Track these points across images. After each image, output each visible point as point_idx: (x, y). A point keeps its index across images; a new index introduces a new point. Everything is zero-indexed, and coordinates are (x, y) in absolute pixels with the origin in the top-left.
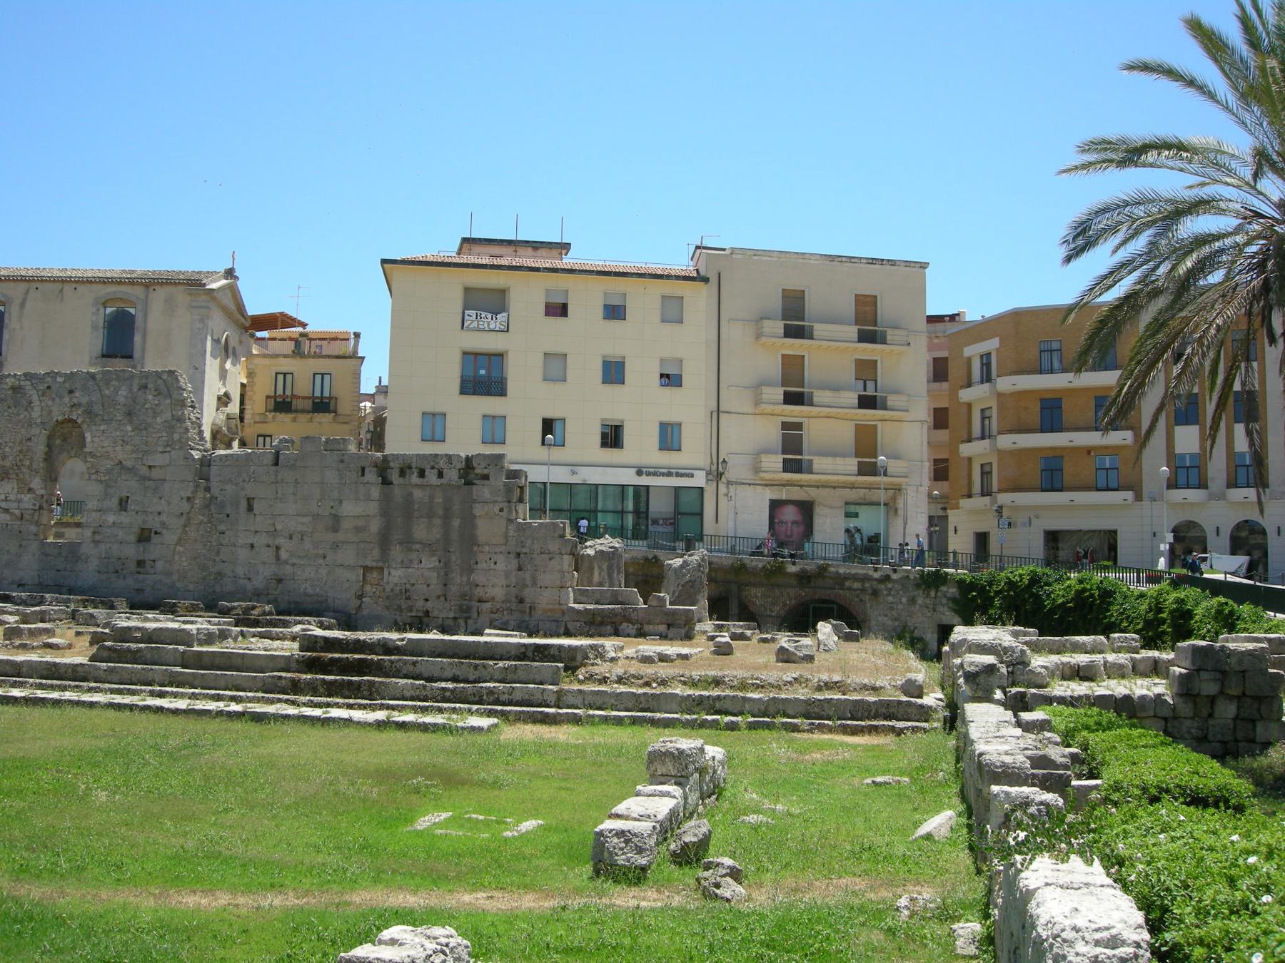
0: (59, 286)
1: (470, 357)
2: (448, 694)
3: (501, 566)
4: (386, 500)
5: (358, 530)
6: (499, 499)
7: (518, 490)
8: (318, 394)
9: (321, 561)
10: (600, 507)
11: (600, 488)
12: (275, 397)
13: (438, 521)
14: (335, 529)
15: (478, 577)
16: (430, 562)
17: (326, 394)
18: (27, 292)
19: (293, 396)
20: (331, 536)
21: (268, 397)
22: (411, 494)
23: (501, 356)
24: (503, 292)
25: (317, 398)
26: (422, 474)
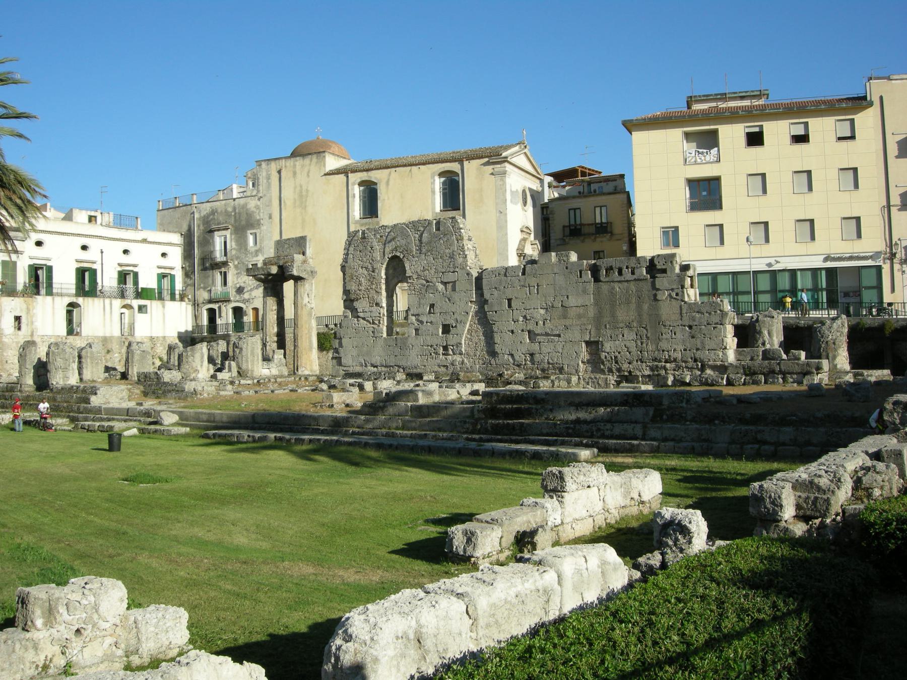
0: (409, 168)
1: (694, 184)
2: (570, 431)
3: (679, 335)
4: (597, 294)
5: (579, 316)
6: (674, 287)
7: (689, 279)
8: (572, 222)
9: (556, 338)
10: (799, 287)
11: (799, 273)
12: (570, 226)
13: (633, 306)
14: (565, 317)
15: (664, 345)
16: (630, 335)
17: (578, 222)
18: (390, 173)
19: (581, 225)
20: (563, 322)
21: (564, 227)
22: (613, 288)
23: (717, 179)
24: (715, 133)
25: (598, 224)
26: (620, 272)
